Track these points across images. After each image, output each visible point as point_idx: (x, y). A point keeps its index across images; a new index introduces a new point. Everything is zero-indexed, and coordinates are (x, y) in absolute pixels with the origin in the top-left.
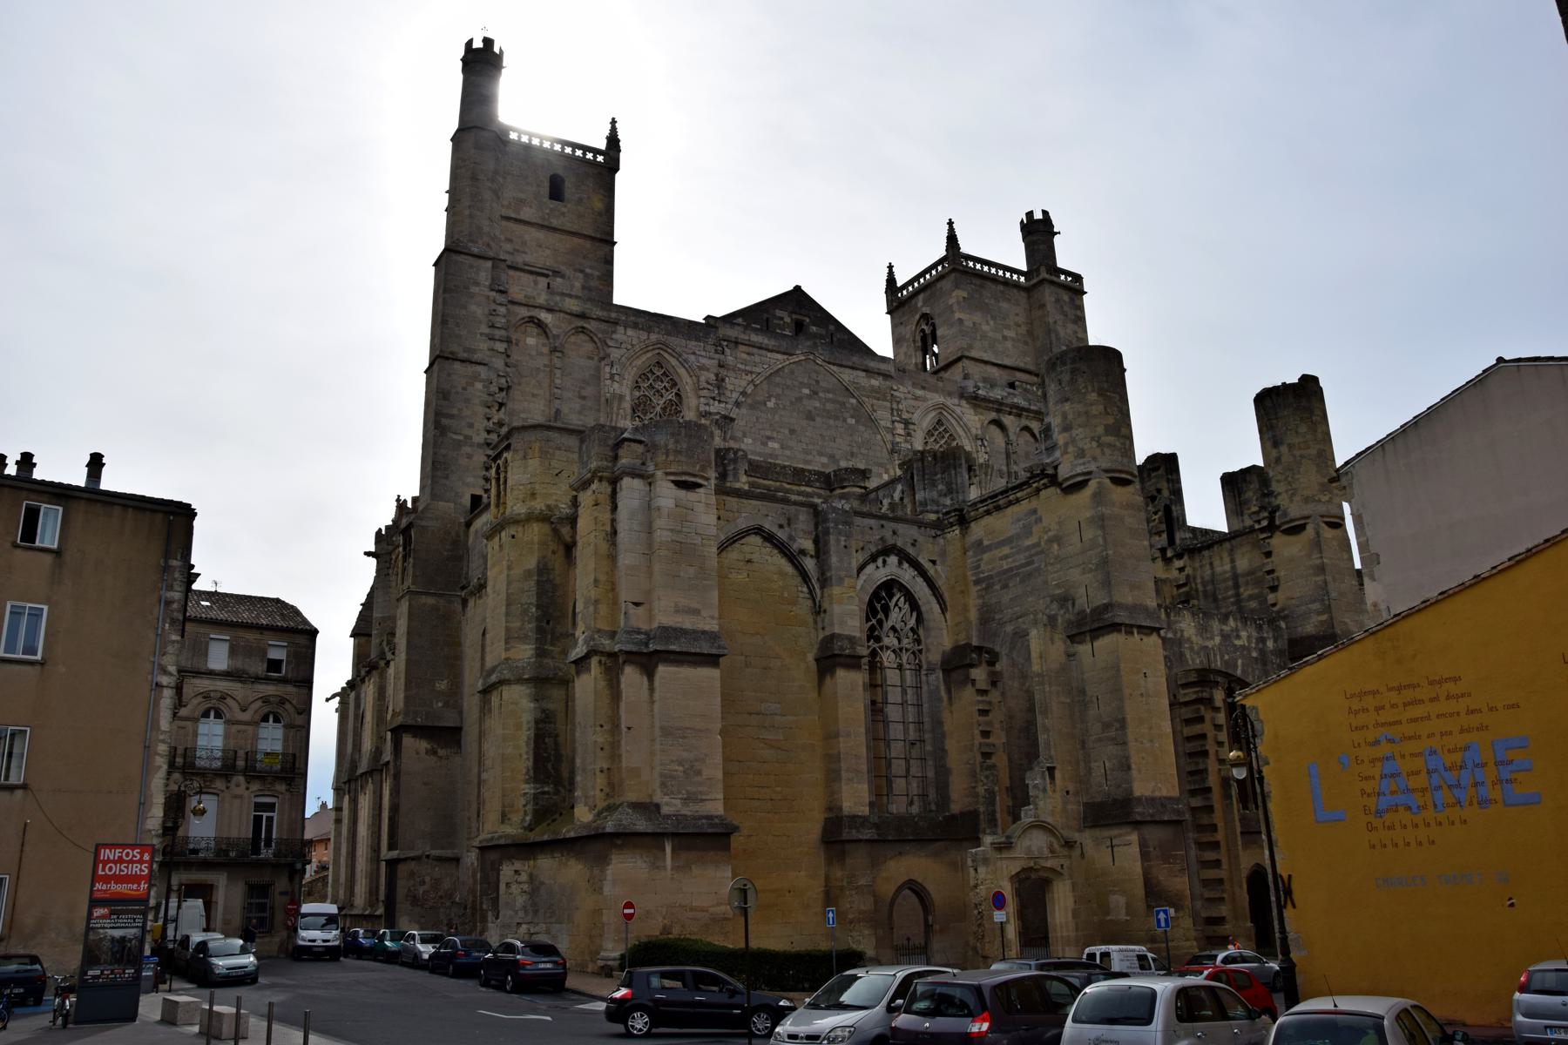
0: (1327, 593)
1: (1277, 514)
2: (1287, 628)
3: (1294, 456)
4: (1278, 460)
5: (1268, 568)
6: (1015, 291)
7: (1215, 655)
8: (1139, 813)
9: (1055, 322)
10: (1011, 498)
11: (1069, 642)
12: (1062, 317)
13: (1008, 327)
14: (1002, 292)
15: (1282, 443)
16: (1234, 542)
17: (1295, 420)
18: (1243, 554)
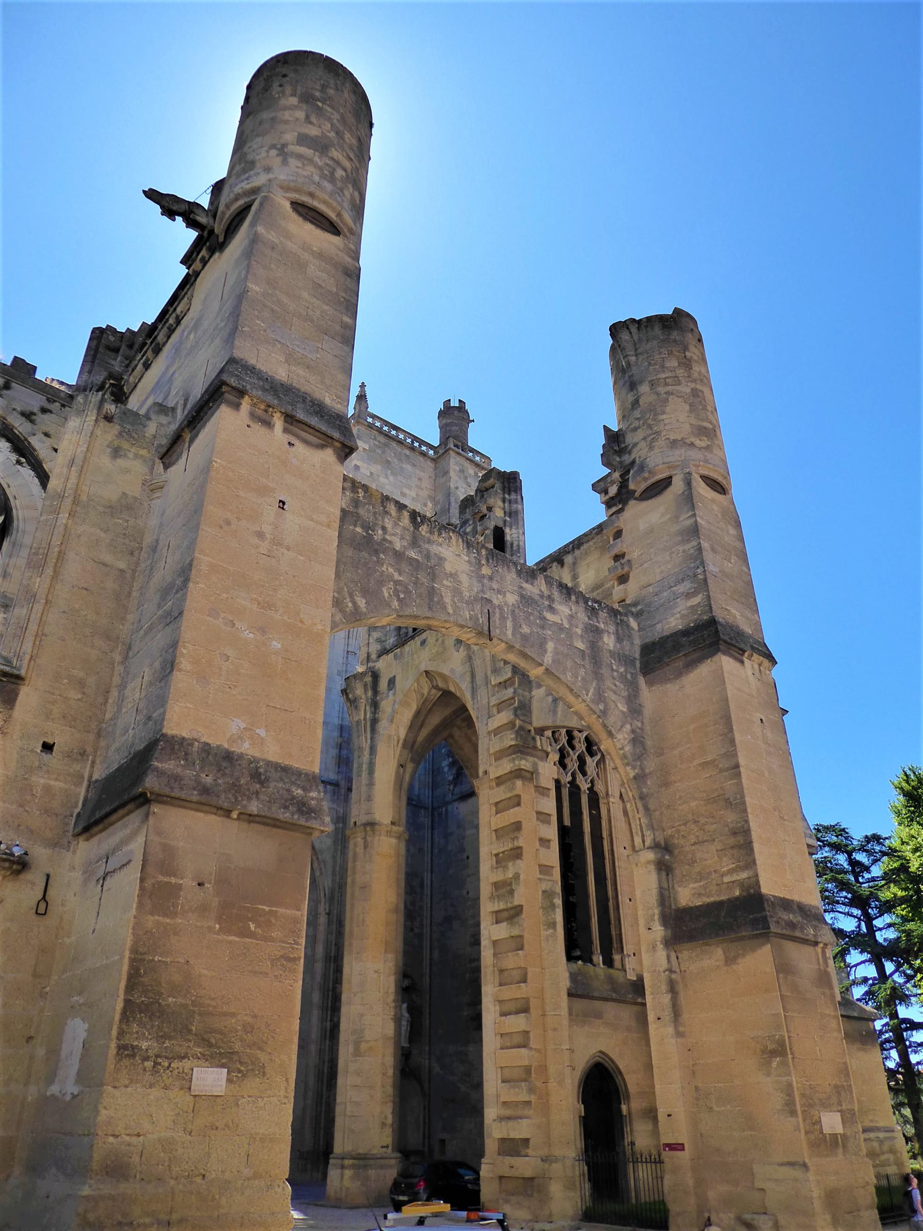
0: (703, 563)
1: (632, 472)
2: (640, 629)
3: (658, 394)
4: (636, 403)
5: (616, 551)
6: (421, 459)
7: (503, 618)
8: (161, 773)
9: (457, 488)
10: (171, 321)
11: (159, 467)
12: (465, 486)
13: (410, 488)
14: (407, 456)
15: (641, 382)
16: (577, 552)
17: (660, 353)
18: (588, 565)
